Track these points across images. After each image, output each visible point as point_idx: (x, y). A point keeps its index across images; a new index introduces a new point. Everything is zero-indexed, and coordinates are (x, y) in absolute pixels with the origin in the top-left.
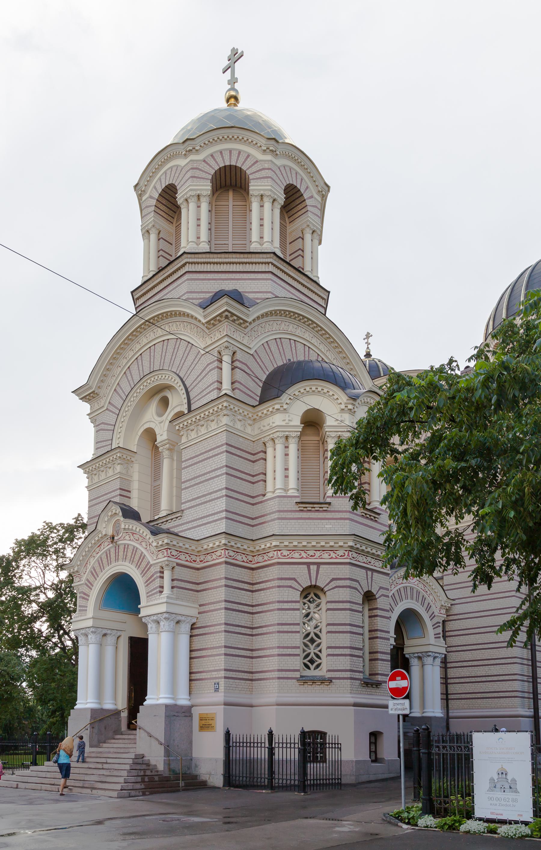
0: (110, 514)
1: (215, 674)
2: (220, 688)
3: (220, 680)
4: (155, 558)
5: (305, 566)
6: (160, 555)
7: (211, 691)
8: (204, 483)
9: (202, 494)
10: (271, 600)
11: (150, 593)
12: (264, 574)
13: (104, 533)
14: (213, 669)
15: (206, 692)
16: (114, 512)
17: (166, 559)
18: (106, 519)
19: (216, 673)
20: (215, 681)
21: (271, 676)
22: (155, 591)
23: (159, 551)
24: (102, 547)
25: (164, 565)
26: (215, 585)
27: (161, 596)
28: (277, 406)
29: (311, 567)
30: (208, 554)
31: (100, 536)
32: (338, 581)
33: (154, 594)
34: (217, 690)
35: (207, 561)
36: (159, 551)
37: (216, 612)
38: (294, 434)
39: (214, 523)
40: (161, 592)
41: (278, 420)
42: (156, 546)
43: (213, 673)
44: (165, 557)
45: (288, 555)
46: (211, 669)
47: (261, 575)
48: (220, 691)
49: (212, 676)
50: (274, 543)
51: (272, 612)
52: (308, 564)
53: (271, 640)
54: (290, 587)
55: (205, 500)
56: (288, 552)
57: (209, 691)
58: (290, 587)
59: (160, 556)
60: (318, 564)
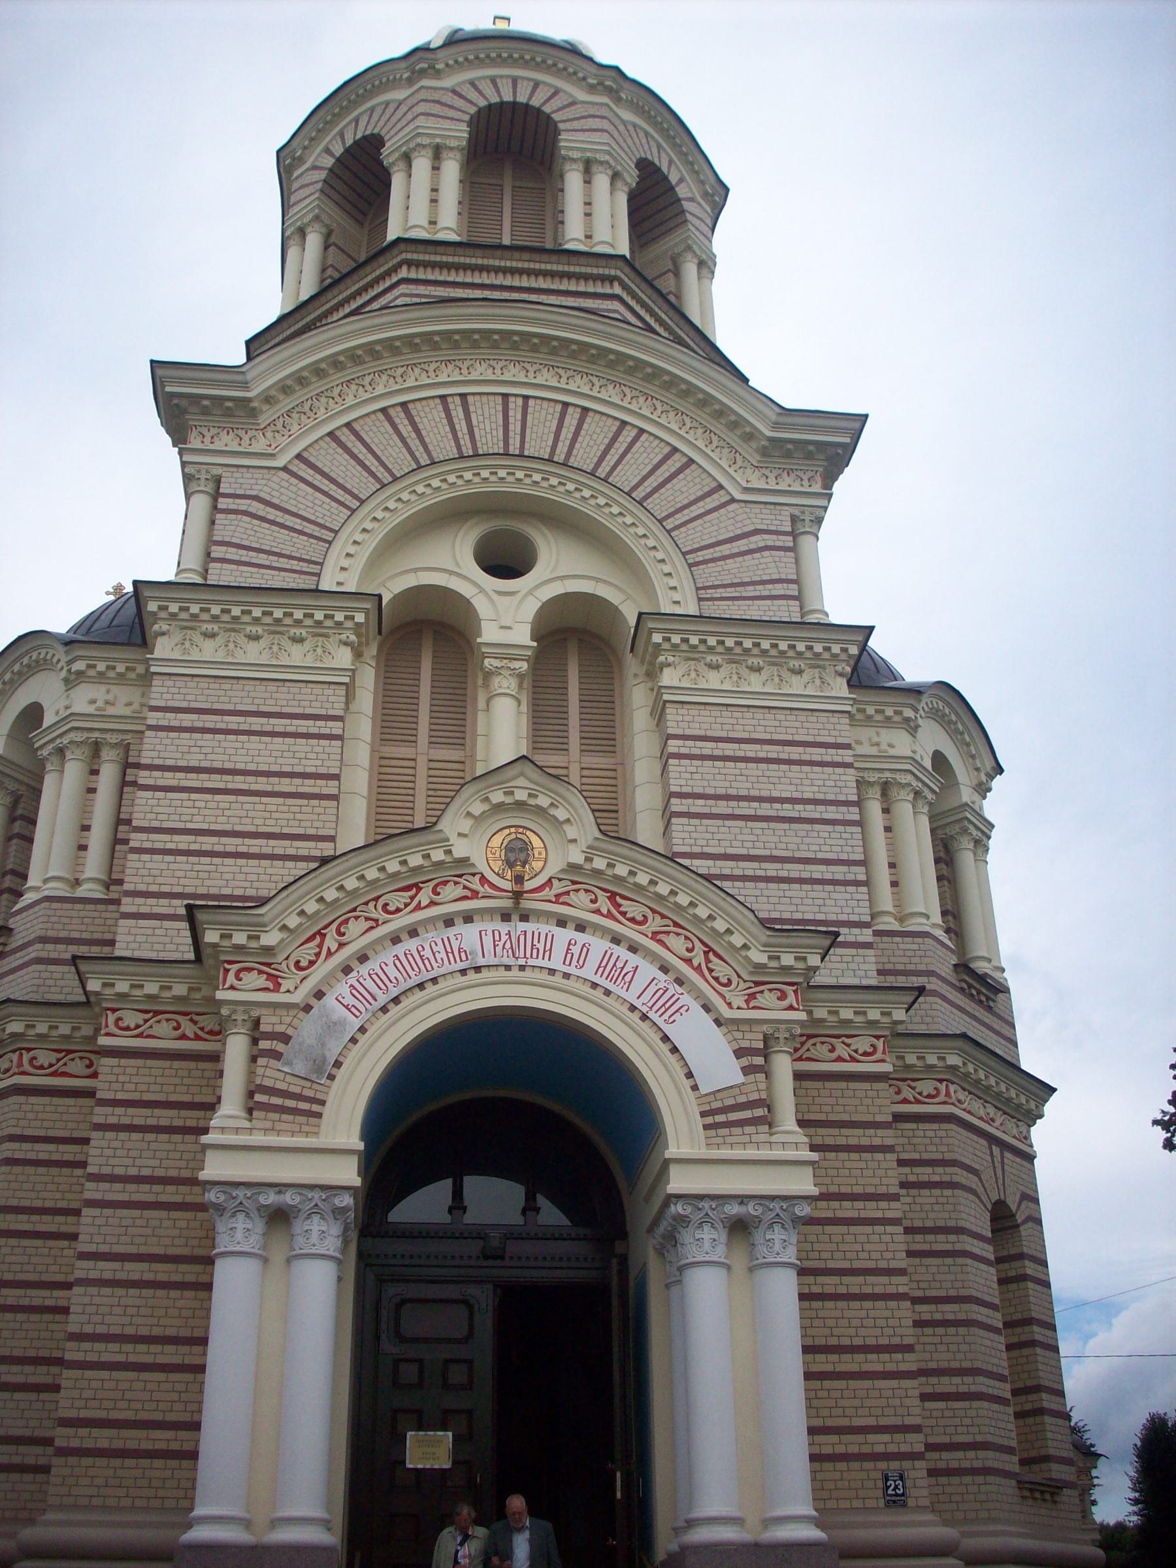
0: (497, 797)
1: (880, 1443)
2: (913, 1492)
3: (907, 1464)
4: (739, 1001)
5: (984, 1142)
6: (768, 998)
7: (870, 1503)
8: (772, 825)
9: (767, 853)
11: (720, 1118)
13: (458, 853)
15: (844, 1504)
16: (521, 795)
17: (802, 1016)
18: (478, 808)
20: (882, 1465)
21: (966, 1464)
22: (747, 1114)
23: (757, 984)
24: (424, 897)
25: (782, 1035)
27: (774, 1138)
28: (908, 713)
31: (438, 855)
34: (896, 1501)
35: (809, 1059)
36: (757, 984)
42: (759, 967)
44: (791, 1008)
48: (911, 1502)
49: (866, 1449)
52: (992, 1139)
53: (953, 1348)
54: (974, 1192)
57: (857, 1504)
58: (974, 1192)
59: (760, 1000)
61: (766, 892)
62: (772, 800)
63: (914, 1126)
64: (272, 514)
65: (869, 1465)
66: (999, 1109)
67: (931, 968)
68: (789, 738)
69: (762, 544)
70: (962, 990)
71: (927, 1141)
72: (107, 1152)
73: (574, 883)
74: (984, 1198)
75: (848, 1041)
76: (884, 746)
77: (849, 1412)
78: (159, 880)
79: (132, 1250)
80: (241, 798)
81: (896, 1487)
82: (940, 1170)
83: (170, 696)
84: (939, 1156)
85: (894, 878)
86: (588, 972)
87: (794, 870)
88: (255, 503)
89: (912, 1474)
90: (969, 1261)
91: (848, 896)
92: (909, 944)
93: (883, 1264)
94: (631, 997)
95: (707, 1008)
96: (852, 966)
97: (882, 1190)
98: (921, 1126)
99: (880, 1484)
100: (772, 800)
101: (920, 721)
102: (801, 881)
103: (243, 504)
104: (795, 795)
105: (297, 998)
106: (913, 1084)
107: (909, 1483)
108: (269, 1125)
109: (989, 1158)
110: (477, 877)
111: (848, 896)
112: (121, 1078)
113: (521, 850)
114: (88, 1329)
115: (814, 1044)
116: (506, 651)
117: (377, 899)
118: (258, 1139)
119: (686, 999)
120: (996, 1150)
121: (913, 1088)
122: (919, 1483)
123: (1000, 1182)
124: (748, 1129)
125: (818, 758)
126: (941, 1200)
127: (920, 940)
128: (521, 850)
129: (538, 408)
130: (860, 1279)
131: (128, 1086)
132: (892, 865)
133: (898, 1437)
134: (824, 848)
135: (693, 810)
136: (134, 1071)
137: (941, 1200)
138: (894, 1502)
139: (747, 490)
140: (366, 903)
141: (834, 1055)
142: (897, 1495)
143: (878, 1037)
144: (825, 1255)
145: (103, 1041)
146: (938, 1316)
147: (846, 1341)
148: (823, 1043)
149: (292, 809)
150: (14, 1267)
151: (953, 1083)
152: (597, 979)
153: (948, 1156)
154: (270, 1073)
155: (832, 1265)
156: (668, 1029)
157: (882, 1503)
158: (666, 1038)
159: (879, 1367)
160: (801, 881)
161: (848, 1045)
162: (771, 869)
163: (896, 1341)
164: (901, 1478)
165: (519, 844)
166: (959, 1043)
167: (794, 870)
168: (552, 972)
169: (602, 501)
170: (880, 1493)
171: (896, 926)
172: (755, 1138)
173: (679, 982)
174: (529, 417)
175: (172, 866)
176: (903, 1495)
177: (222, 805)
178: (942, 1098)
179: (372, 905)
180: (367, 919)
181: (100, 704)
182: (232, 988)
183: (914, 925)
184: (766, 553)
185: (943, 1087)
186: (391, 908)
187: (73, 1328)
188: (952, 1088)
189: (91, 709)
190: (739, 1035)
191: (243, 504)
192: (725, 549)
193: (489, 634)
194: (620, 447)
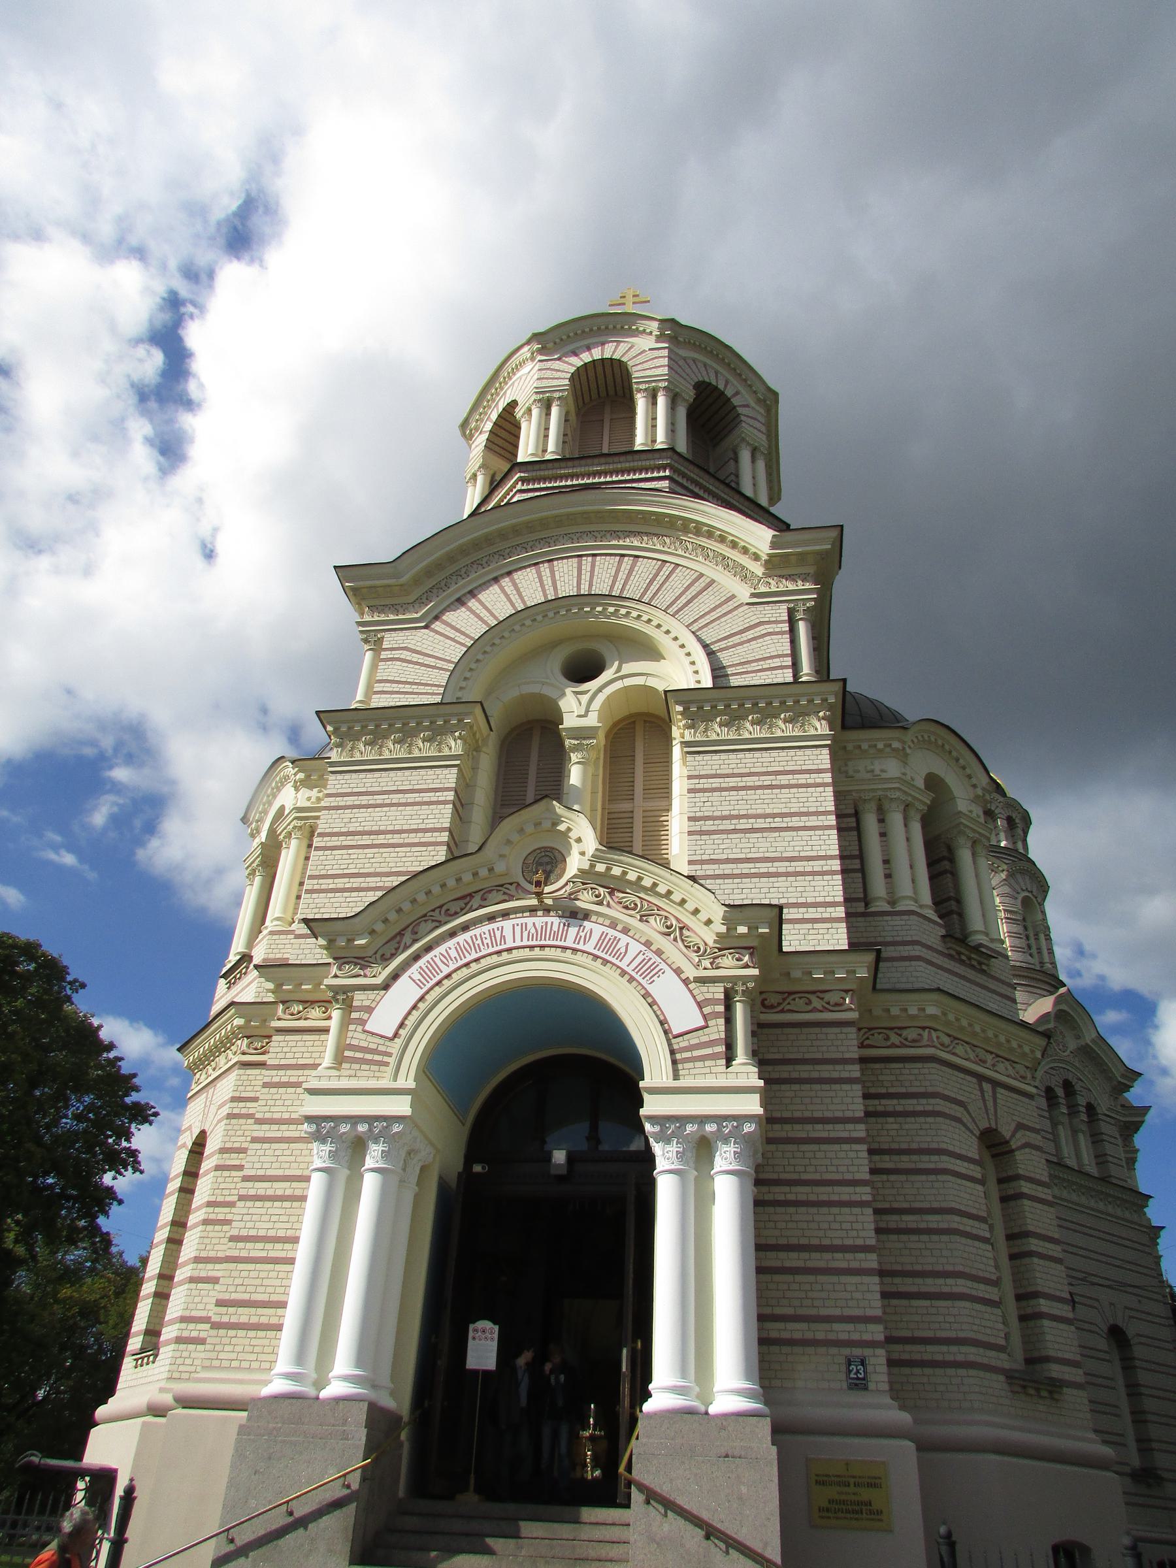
1: (843, 1331)
2: (873, 1378)
3: (867, 1352)
4: (706, 963)
5: (974, 1080)
8: (765, 834)
9: (761, 855)
10: (925, 1146)
12: (893, 1078)
14: (837, 1312)
19: (850, 1327)
20: (846, 1351)
21: (950, 1358)
22: (709, 1051)
25: (740, 988)
26: (805, 1075)
28: (896, 745)
29: (984, 1085)
30: (790, 993)
32: (1028, 1133)
33: (702, 1058)
34: (859, 1384)
37: (837, 1147)
38: (921, 807)
39: (809, 926)
40: (729, 1059)
41: (892, 768)
43: (836, 1326)
44: (746, 966)
45: (949, 1046)
46: (824, 1312)
47: (881, 1078)
48: (872, 1386)
49: (832, 1336)
50: (931, 1010)
51: (933, 1177)
52: (981, 1078)
55: (772, 870)
56: (946, 1040)
60: (995, 1084)
61: (758, 885)
62: (765, 816)
63: (901, 1065)
64: (416, 657)
65: (833, 1350)
66: (991, 1053)
67: (915, 938)
68: (781, 769)
69: (765, 632)
70: (950, 957)
71: (912, 1077)
72: (270, 1102)
73: (584, 884)
74: (971, 1126)
75: (821, 995)
76: (877, 772)
77: (816, 1303)
78: (322, 910)
79: (280, 1173)
80: (382, 850)
81: (858, 1371)
82: (924, 1101)
83: (339, 786)
84: (922, 1090)
85: (887, 872)
86: (589, 947)
87: (781, 867)
88: (405, 652)
89: (873, 1361)
90: (949, 1178)
91: (825, 883)
92: (897, 921)
93: (848, 1177)
94: (623, 965)
95: (678, 972)
96: (826, 937)
97: (849, 1114)
98: (907, 1065)
99: (844, 1368)
100: (765, 816)
101: (908, 751)
102: (787, 874)
103: (397, 654)
104: (784, 811)
105: (379, 980)
106: (899, 1032)
107: (870, 1369)
108: (352, 1073)
109: (979, 1093)
110: (515, 885)
111: (825, 883)
112: (285, 1050)
113: (547, 863)
114: (244, 1233)
115: (794, 999)
116: (581, 733)
117: (441, 907)
118: (344, 1083)
119: (663, 966)
120: (987, 1087)
121: (900, 1035)
122: (878, 1369)
123: (992, 1111)
124: (708, 1063)
125: (804, 781)
126: (924, 1126)
127: (906, 917)
128: (547, 863)
129: (603, 561)
130: (829, 1189)
131: (288, 1055)
132: (886, 862)
133: (861, 1327)
134: (806, 848)
135: (704, 828)
136: (294, 1044)
137: (924, 1126)
138: (856, 1385)
139: (753, 595)
140: (433, 910)
141: (810, 1008)
142: (858, 1379)
143: (846, 991)
144: (799, 1169)
145: (275, 1024)
146: (923, 1225)
147: (815, 1242)
148: (800, 998)
149: (416, 854)
150: (225, 1192)
151: (935, 1030)
152: (596, 952)
153: (930, 1090)
154: (356, 1036)
155: (805, 1177)
156: (650, 988)
157: (845, 1385)
158: (646, 995)
159: (844, 1265)
160: (787, 874)
161: (822, 999)
162: (763, 868)
163: (860, 1242)
164: (863, 1363)
165: (546, 859)
166: (935, 996)
167: (781, 867)
168: (565, 948)
169: (611, 609)
170: (843, 1377)
171: (887, 908)
172: (714, 1070)
173: (659, 953)
174: (597, 568)
175: (332, 900)
176: (864, 1379)
177: (368, 856)
178: (925, 1042)
179: (437, 911)
180: (433, 921)
181: (313, 799)
182: (336, 976)
183: (900, 907)
184: (768, 638)
185: (926, 1034)
186: (452, 911)
187: (235, 1232)
188: (934, 1035)
189: (308, 804)
190: (704, 989)
191: (397, 654)
192: (736, 639)
193: (570, 721)
194: (661, 579)
